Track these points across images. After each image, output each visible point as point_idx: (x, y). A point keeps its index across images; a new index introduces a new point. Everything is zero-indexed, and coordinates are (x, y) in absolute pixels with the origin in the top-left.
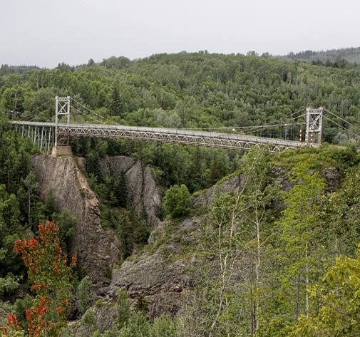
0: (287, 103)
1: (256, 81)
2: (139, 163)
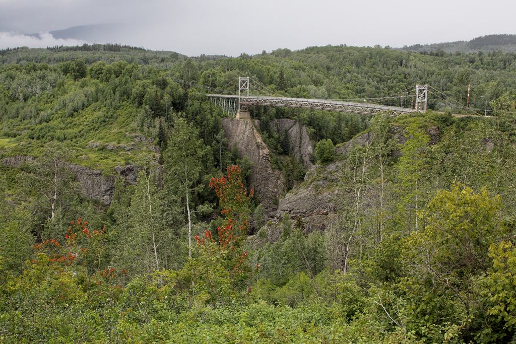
0: (402, 81)
1: (381, 66)
2: (298, 124)
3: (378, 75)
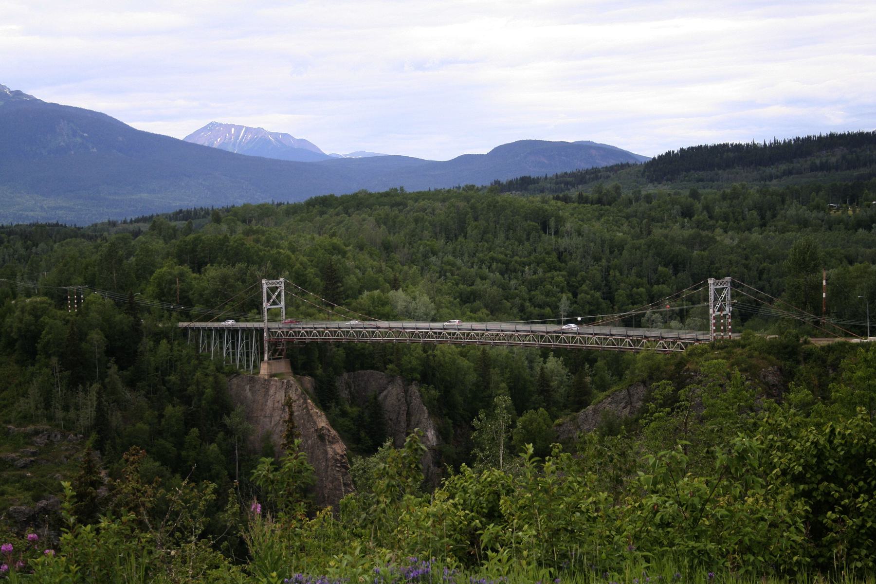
0: (556, 269)
1: (502, 236)
3: (501, 256)
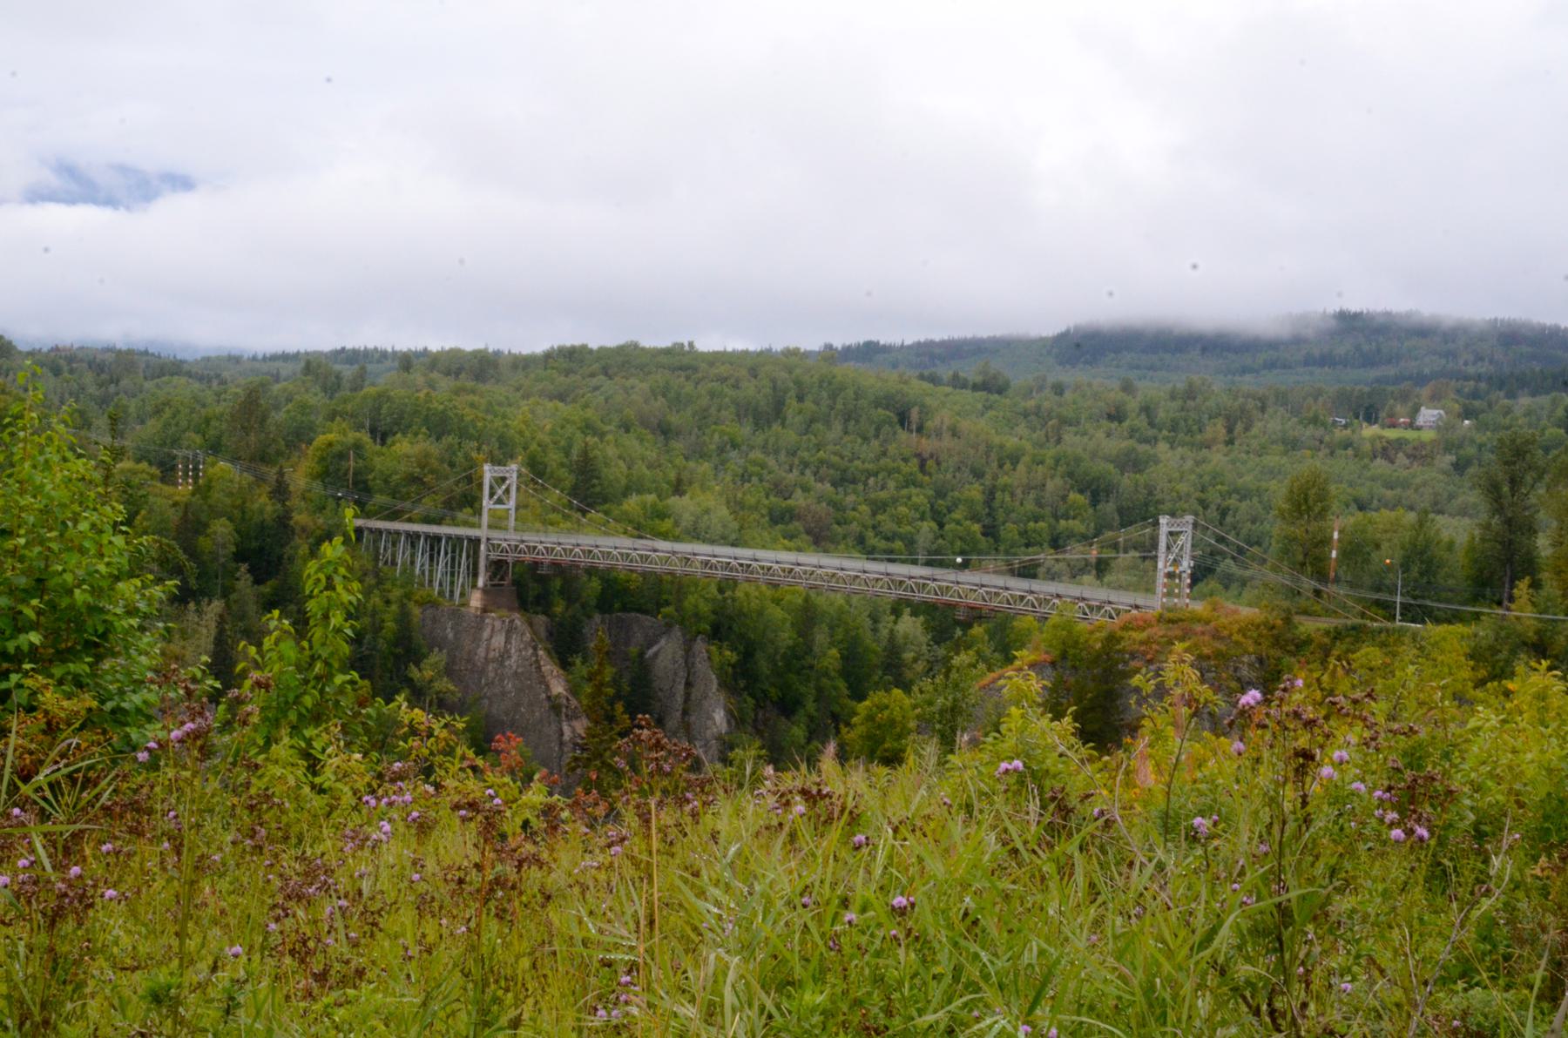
0: (916, 485)
1: (838, 427)
2: (677, 632)
3: (835, 459)
